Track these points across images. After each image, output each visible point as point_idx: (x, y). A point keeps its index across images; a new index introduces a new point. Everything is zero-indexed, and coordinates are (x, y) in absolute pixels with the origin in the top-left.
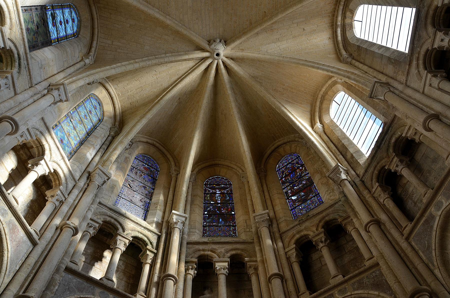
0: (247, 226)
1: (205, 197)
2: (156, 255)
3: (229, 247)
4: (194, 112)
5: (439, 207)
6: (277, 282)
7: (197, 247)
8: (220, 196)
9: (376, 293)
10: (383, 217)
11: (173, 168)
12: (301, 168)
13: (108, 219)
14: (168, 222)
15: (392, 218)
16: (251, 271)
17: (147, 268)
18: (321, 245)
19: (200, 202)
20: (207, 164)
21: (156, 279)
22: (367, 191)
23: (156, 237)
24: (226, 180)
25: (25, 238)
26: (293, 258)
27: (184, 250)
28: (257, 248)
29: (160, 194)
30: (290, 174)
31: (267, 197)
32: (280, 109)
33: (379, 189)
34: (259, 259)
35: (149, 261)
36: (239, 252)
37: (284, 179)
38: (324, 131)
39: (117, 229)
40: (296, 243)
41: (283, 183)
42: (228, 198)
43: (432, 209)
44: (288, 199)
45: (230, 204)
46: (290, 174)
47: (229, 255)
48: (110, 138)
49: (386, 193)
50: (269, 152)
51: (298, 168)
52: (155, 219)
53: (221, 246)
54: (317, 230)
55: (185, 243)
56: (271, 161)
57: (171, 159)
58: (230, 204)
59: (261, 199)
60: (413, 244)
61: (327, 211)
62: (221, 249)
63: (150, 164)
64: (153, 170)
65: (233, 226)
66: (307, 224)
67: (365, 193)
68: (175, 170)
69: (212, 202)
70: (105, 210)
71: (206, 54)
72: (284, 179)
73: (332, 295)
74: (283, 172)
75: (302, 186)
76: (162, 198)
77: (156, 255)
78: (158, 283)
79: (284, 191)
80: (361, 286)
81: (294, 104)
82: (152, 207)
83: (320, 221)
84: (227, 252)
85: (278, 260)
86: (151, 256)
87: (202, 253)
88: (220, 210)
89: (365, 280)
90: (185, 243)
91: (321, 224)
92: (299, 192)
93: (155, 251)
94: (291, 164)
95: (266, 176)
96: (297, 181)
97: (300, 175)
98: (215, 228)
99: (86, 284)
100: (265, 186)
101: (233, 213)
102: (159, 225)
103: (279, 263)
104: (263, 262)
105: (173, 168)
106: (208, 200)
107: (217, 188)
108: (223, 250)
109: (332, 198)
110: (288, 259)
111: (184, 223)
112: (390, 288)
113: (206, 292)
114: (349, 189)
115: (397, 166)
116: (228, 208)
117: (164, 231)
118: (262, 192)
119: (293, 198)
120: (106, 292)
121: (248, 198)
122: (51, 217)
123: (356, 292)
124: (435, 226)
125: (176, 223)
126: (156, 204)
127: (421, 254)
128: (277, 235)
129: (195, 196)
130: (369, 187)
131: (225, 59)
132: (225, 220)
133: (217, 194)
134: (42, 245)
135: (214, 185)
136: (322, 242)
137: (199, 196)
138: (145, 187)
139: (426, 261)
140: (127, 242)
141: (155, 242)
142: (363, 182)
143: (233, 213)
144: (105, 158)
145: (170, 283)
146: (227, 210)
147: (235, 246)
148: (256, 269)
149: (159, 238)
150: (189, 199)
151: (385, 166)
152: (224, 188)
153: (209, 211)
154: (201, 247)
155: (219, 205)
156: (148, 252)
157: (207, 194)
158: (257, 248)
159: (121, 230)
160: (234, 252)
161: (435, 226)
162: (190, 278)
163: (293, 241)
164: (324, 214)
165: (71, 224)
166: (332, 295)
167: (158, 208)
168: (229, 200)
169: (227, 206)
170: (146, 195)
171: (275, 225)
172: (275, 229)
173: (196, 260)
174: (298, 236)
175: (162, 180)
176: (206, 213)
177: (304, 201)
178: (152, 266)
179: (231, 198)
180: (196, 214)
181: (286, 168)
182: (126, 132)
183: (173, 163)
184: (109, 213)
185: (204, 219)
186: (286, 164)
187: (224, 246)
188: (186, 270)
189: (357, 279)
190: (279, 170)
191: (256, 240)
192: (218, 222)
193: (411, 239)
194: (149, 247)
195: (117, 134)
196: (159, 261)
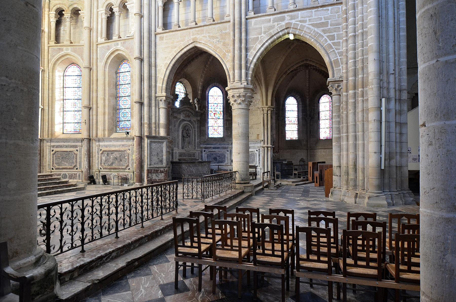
5: (67, 50)
15: (49, 32)
22: (48, 10)
43: (65, 48)
60: (50, 49)
115: (68, 18)
124: (61, 53)
127: (50, 55)
130: (51, 8)
139: (49, 59)
151: (64, 11)
161: (61, 53)
193: (50, 47)
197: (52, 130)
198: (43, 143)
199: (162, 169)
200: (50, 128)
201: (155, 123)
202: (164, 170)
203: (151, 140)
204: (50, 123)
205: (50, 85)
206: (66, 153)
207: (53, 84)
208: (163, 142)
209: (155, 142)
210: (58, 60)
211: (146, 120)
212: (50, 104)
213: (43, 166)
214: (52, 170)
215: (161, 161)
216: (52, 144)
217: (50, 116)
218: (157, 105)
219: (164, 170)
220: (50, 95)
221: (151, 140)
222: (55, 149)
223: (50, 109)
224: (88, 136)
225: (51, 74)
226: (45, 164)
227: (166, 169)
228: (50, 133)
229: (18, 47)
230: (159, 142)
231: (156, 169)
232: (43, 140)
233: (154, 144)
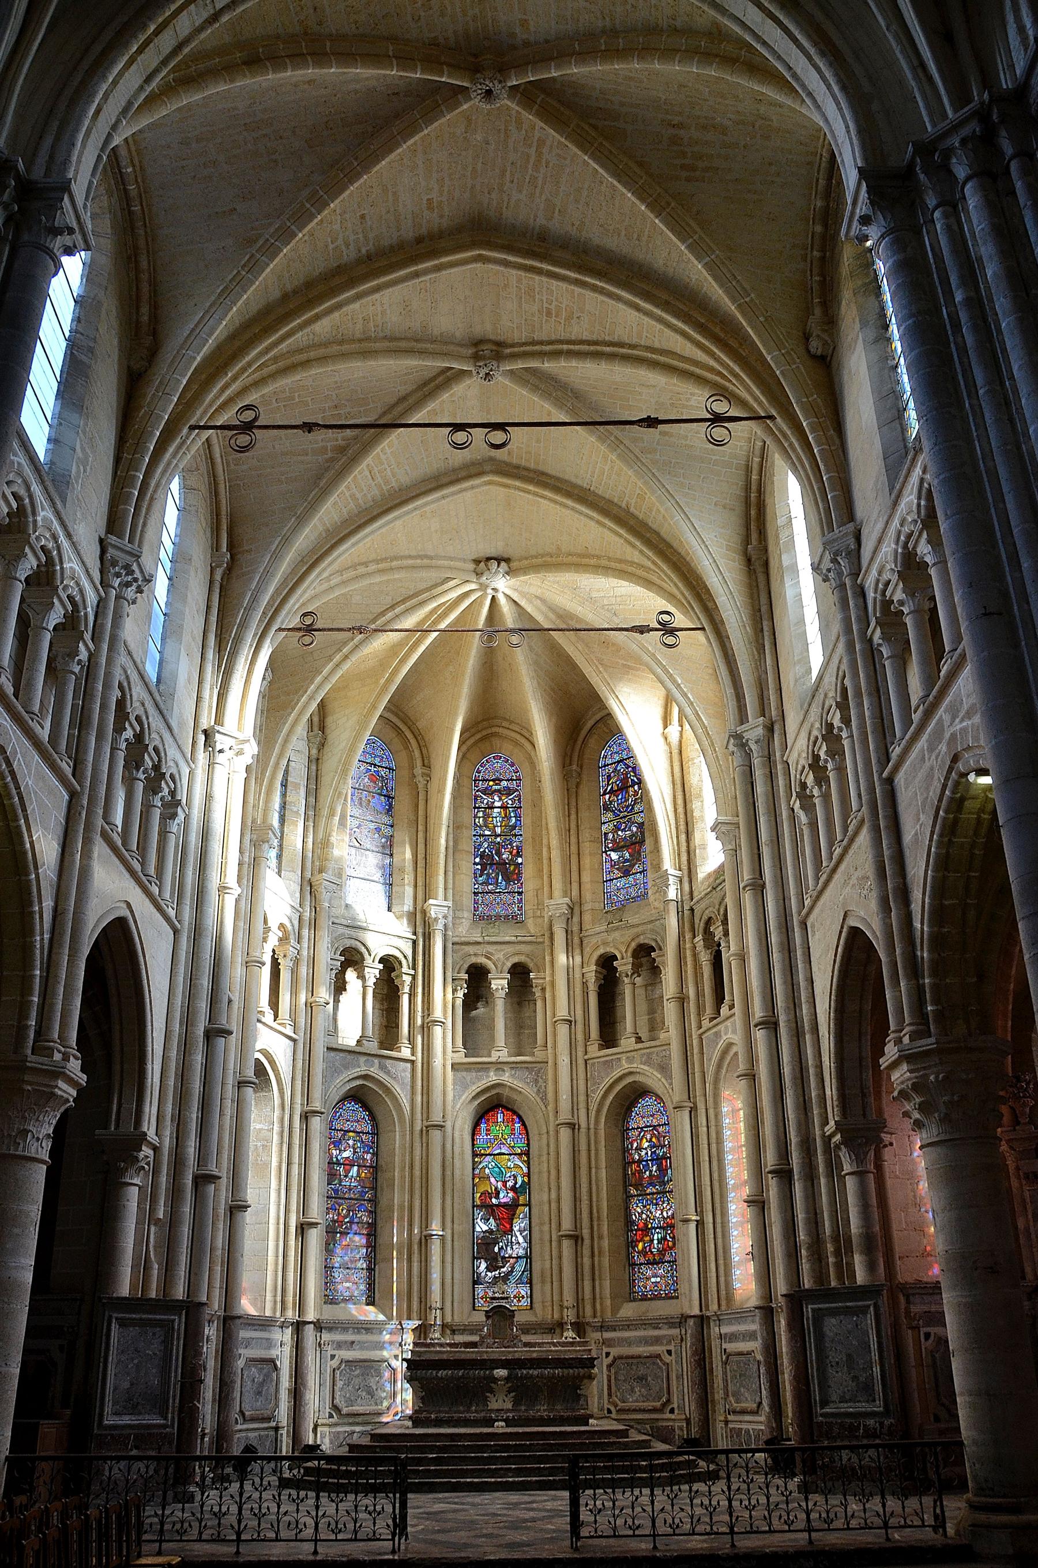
0: (538, 904)
1: (476, 817)
2: (414, 977)
3: (510, 949)
4: (451, 668)
6: (563, 1030)
7: (467, 948)
8: (500, 813)
9: (659, 1076)
10: (692, 992)
11: (419, 770)
12: (636, 787)
13: (349, 943)
14: (424, 912)
15: (699, 994)
16: (538, 994)
17: (405, 1000)
18: (626, 980)
19: (467, 845)
20: (478, 736)
21: (419, 1022)
23: (410, 944)
24: (512, 765)
25: (287, 1041)
26: (592, 987)
27: (449, 961)
28: (548, 958)
29: (403, 843)
30: (620, 789)
31: (574, 848)
32: (607, 699)
33: (702, 943)
34: (548, 979)
35: (407, 989)
36: (522, 959)
37: (607, 797)
38: (680, 742)
39: (363, 959)
40: (597, 964)
41: (606, 808)
42: (514, 820)
44: (606, 852)
45: (516, 835)
46: (620, 789)
47: (509, 964)
48: (314, 768)
49: (709, 952)
50: (590, 724)
51: (634, 783)
52: (406, 908)
53: (498, 947)
54: (626, 952)
55: (450, 945)
56: (592, 742)
57: (413, 741)
58: (516, 835)
59: (562, 857)
61: (645, 927)
62: (499, 956)
63: (377, 761)
64: (383, 772)
65: (520, 893)
66: (616, 935)
67: (688, 936)
68: (423, 774)
69: (487, 833)
70: (341, 930)
71: (473, 586)
72: (607, 797)
73: (619, 1059)
74: (609, 778)
75: (631, 837)
76: (408, 855)
77: (414, 977)
78: (422, 1026)
79: (604, 828)
80: (648, 1062)
81: (638, 669)
82: (396, 879)
83: (633, 940)
84: (507, 959)
85: (571, 988)
86: (407, 979)
87: (474, 960)
88: (499, 853)
89: (654, 1056)
90: (450, 945)
91: (633, 945)
92: (623, 847)
93: (412, 972)
94: (625, 764)
95: (578, 785)
96: (624, 817)
97: (633, 808)
98: (492, 897)
99: (349, 1057)
100: (573, 817)
101: (520, 860)
102: (412, 917)
103: (571, 993)
104: (553, 984)
105: (419, 770)
106: (480, 827)
107: (496, 791)
108: (501, 955)
109: (656, 904)
110: (585, 984)
111: (445, 917)
112: (671, 1078)
113: (479, 1004)
114: (672, 921)
116: (512, 847)
117: (420, 930)
118: (566, 833)
119: (614, 856)
120: (370, 1058)
121: (545, 841)
122: (294, 992)
123: (642, 1066)
125: (436, 919)
126: (402, 870)
128: (576, 940)
129: (458, 827)
131: (509, 592)
132: (508, 879)
133: (496, 810)
134: (300, 1037)
135: (491, 783)
136: (627, 976)
137: (467, 828)
138: (378, 830)
140: (377, 972)
141: (409, 953)
142: (692, 910)
143: (520, 860)
144: (320, 835)
145: (438, 1031)
146: (511, 853)
147: (518, 947)
148: (543, 990)
149: (414, 942)
150: (451, 843)
152: (508, 792)
153: (482, 856)
154: (471, 949)
155: (498, 839)
156: (405, 977)
157: (479, 808)
158: (548, 958)
159: (366, 955)
160: (516, 959)
162: (459, 1002)
163: (595, 957)
164: (640, 929)
165: (321, 1000)
166: (619, 1059)
167: (406, 881)
168: (514, 827)
169: (510, 844)
170: (383, 847)
171: (576, 919)
172: (576, 929)
173: (466, 977)
174: (601, 951)
175: (403, 803)
176: (477, 860)
177: (626, 873)
178: (412, 995)
179: (518, 817)
180: (462, 876)
181: (615, 769)
182: (340, 761)
183: (417, 753)
184: (348, 932)
185: (475, 877)
186: (617, 758)
187: (503, 947)
188: (454, 991)
189: (648, 1051)
190: (605, 766)
191: (547, 942)
192: (497, 883)
194: (405, 969)
195: (322, 746)
196: (420, 990)
197: (728, 1284)
198: (709, 1328)
199: (871, 1422)
200: (722, 1279)
201: (836, 1238)
202: (882, 1424)
203: (816, 1306)
204: (721, 1262)
205: (714, 1146)
206: (742, 1358)
207: (720, 1141)
208: (864, 1311)
209: (834, 1313)
210: (719, 1066)
211: (802, 1236)
212: (718, 1205)
213: (713, 1401)
214: (730, 1418)
215: (867, 1389)
216: (726, 1329)
217: (720, 1241)
218: (833, 1167)
219: (882, 1424)
220: (716, 1176)
221: (816, 1306)
222: (731, 1347)
223: (718, 1220)
224: (762, 1298)
225: (711, 1112)
226: (716, 1397)
227: (887, 1422)
228: (723, 1293)
229: (975, 979)
230: (848, 1312)
231: (848, 1421)
232: (708, 1318)
233: (833, 1321)
